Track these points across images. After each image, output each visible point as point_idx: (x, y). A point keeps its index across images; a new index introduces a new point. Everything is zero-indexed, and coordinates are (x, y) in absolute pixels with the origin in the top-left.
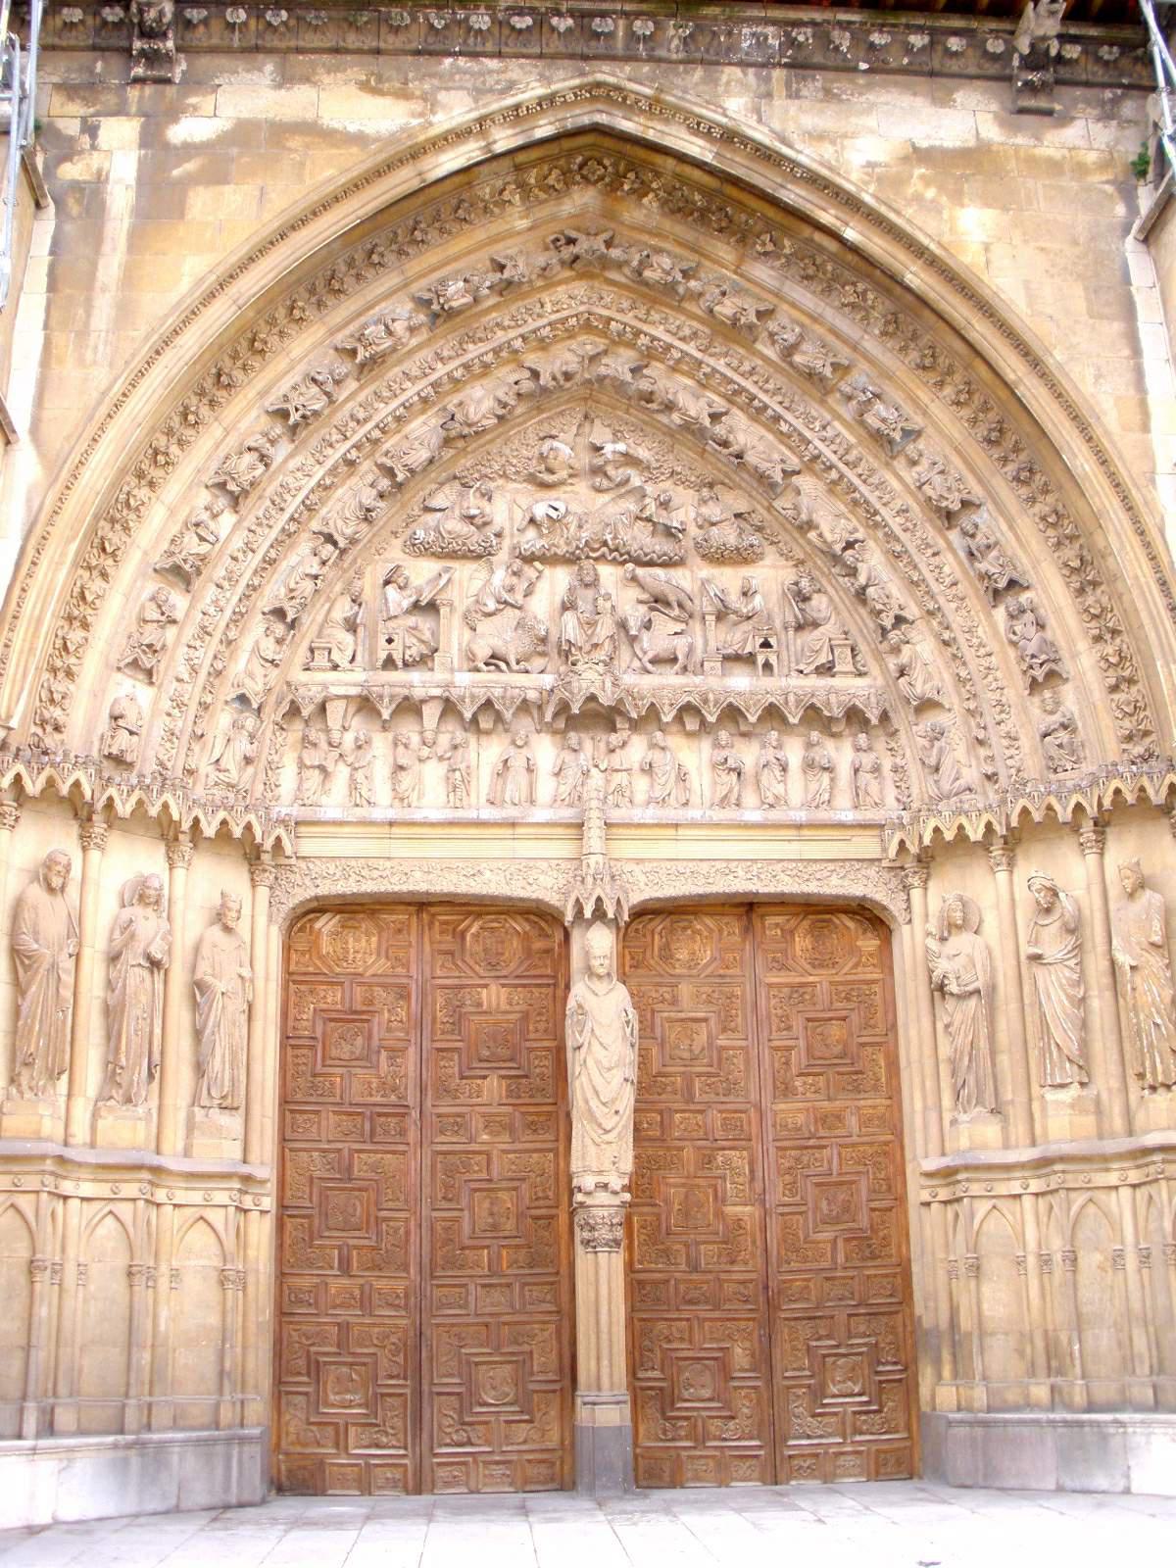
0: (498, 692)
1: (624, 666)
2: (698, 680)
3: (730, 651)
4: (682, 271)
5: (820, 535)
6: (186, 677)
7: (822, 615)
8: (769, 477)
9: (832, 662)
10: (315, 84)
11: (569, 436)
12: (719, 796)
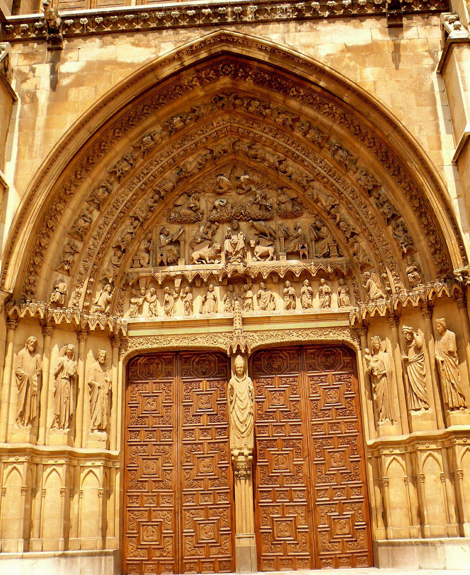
0: (201, 272)
3: (289, 250)
4: (263, 106)
5: (322, 204)
6: (83, 272)
9: (329, 253)
10: (115, 45)
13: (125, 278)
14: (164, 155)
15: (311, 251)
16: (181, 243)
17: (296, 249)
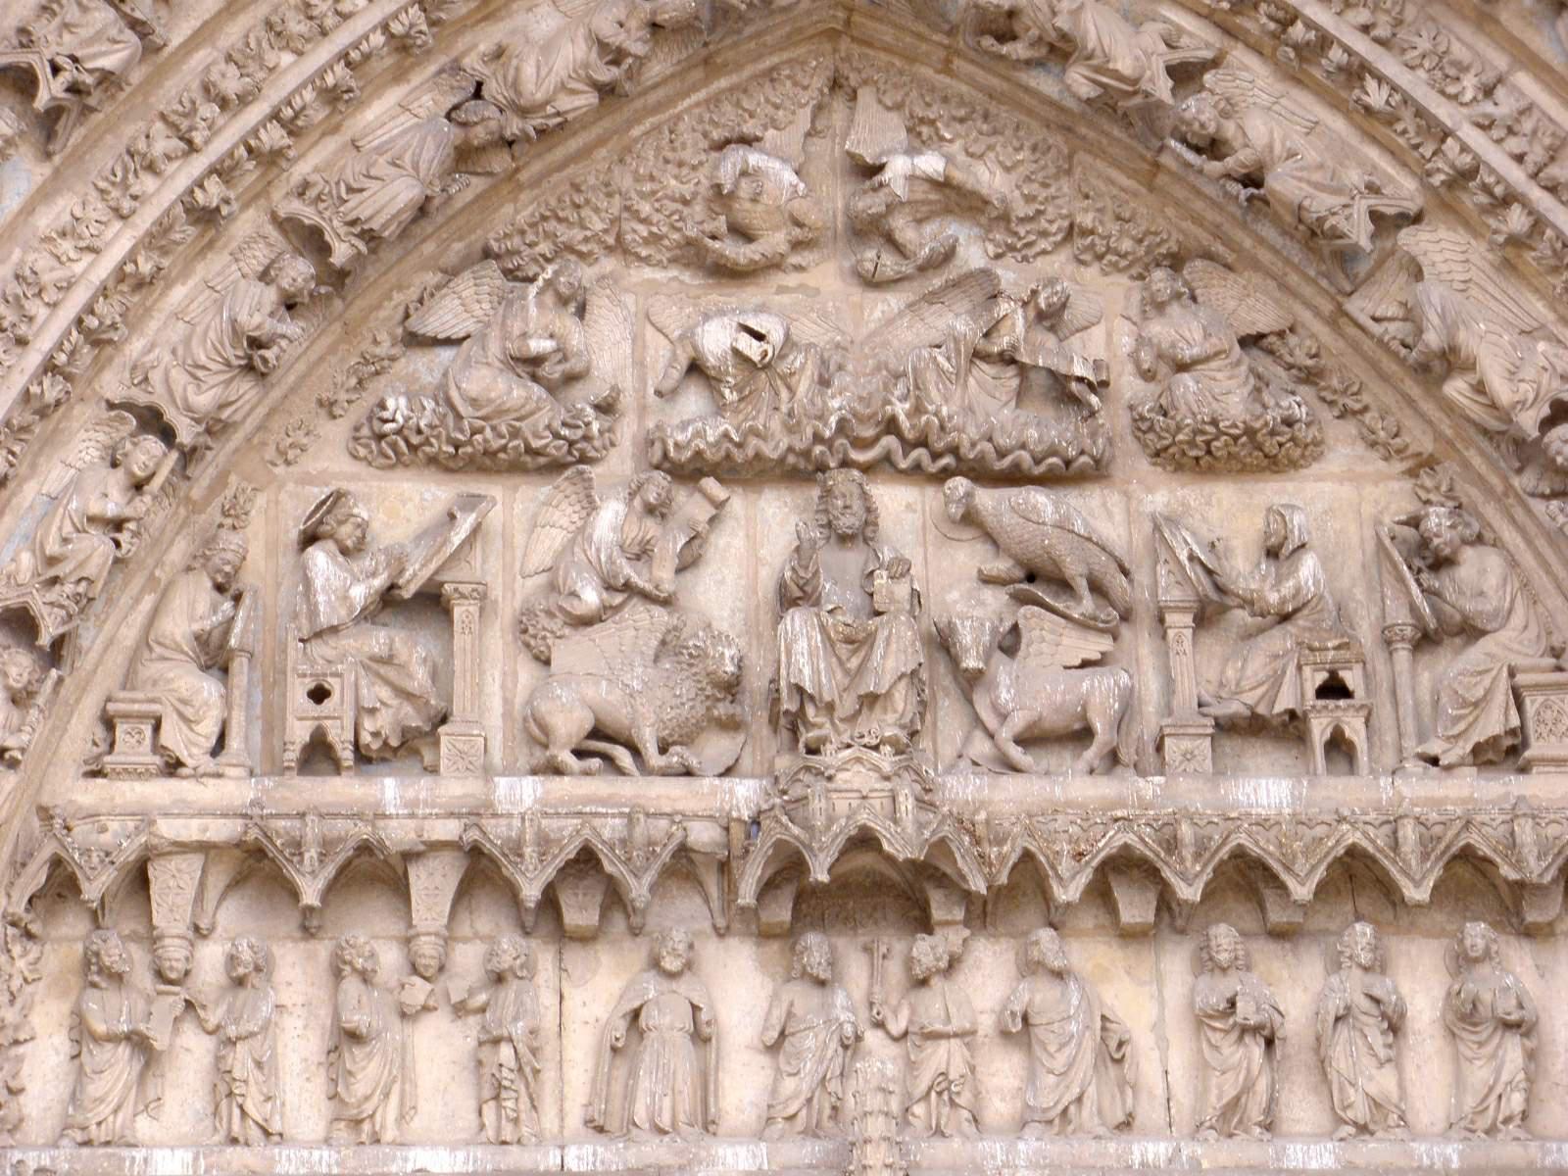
0: (611, 828)
1: (948, 751)
2: (1150, 786)
3: (1235, 708)
5: (1480, 388)
7: (1488, 607)
8: (1336, 234)
11: (791, 137)
12: (1215, 1102)
13: (48, 850)
15: (1384, 714)
16: (458, 613)
17: (1285, 701)
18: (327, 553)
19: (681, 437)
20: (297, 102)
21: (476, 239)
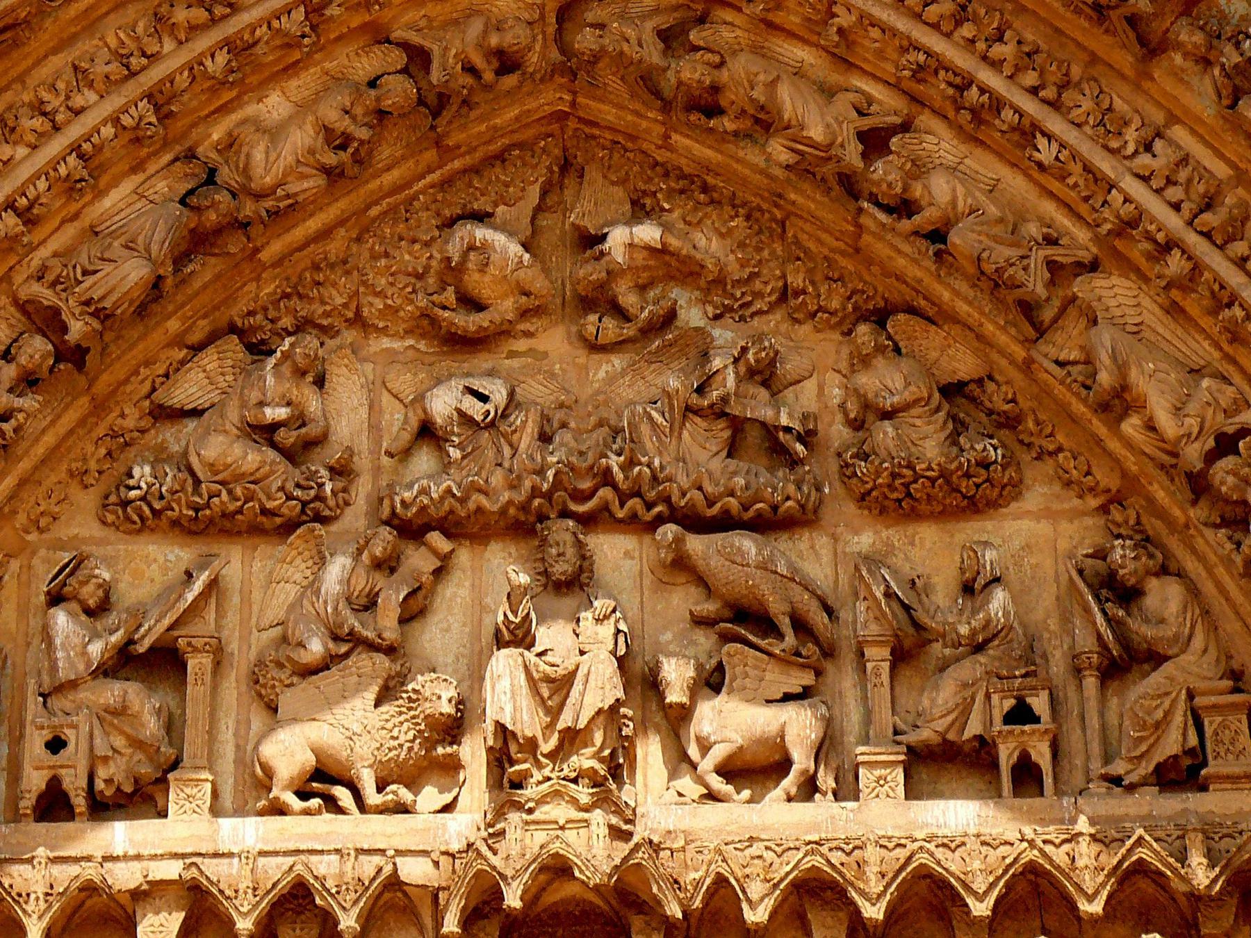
0: (325, 866)
3: (926, 734)
5: (1151, 427)
9: (1198, 756)
14: (100, 69)
15: (1073, 739)
16: (192, 664)
17: (974, 727)
18: (70, 613)
19: (407, 495)
20: (31, 193)
21: (222, 318)
